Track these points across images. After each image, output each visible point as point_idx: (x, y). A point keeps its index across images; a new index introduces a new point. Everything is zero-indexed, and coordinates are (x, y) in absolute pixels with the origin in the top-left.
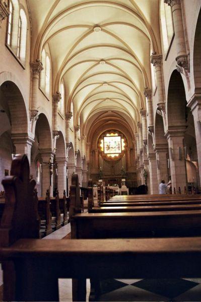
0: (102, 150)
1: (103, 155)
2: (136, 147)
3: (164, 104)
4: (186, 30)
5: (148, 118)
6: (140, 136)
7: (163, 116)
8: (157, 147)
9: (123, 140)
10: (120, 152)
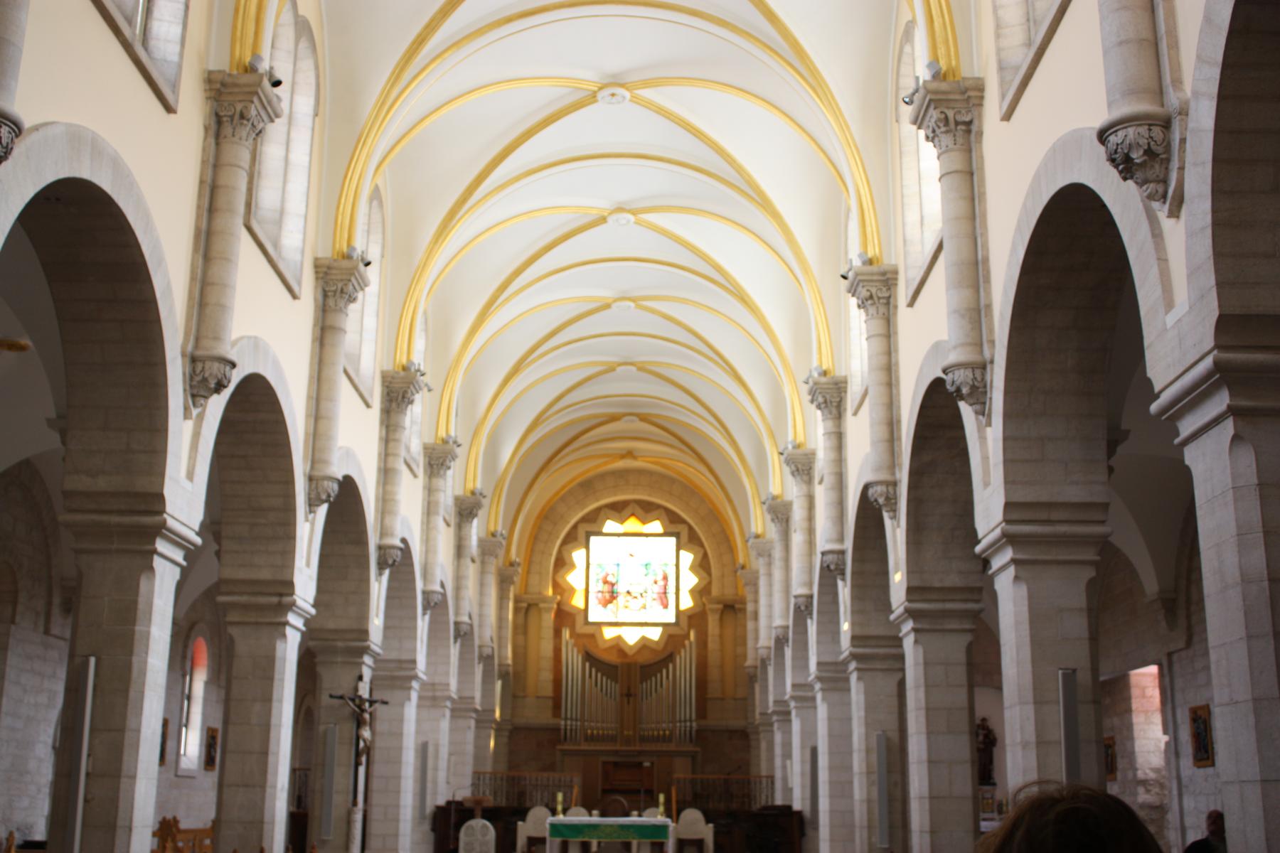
0: (578, 601)
1: (580, 628)
2: (756, 601)
3: (895, 484)
4: (986, 260)
5: (822, 495)
9: (687, 558)
10: (671, 618)
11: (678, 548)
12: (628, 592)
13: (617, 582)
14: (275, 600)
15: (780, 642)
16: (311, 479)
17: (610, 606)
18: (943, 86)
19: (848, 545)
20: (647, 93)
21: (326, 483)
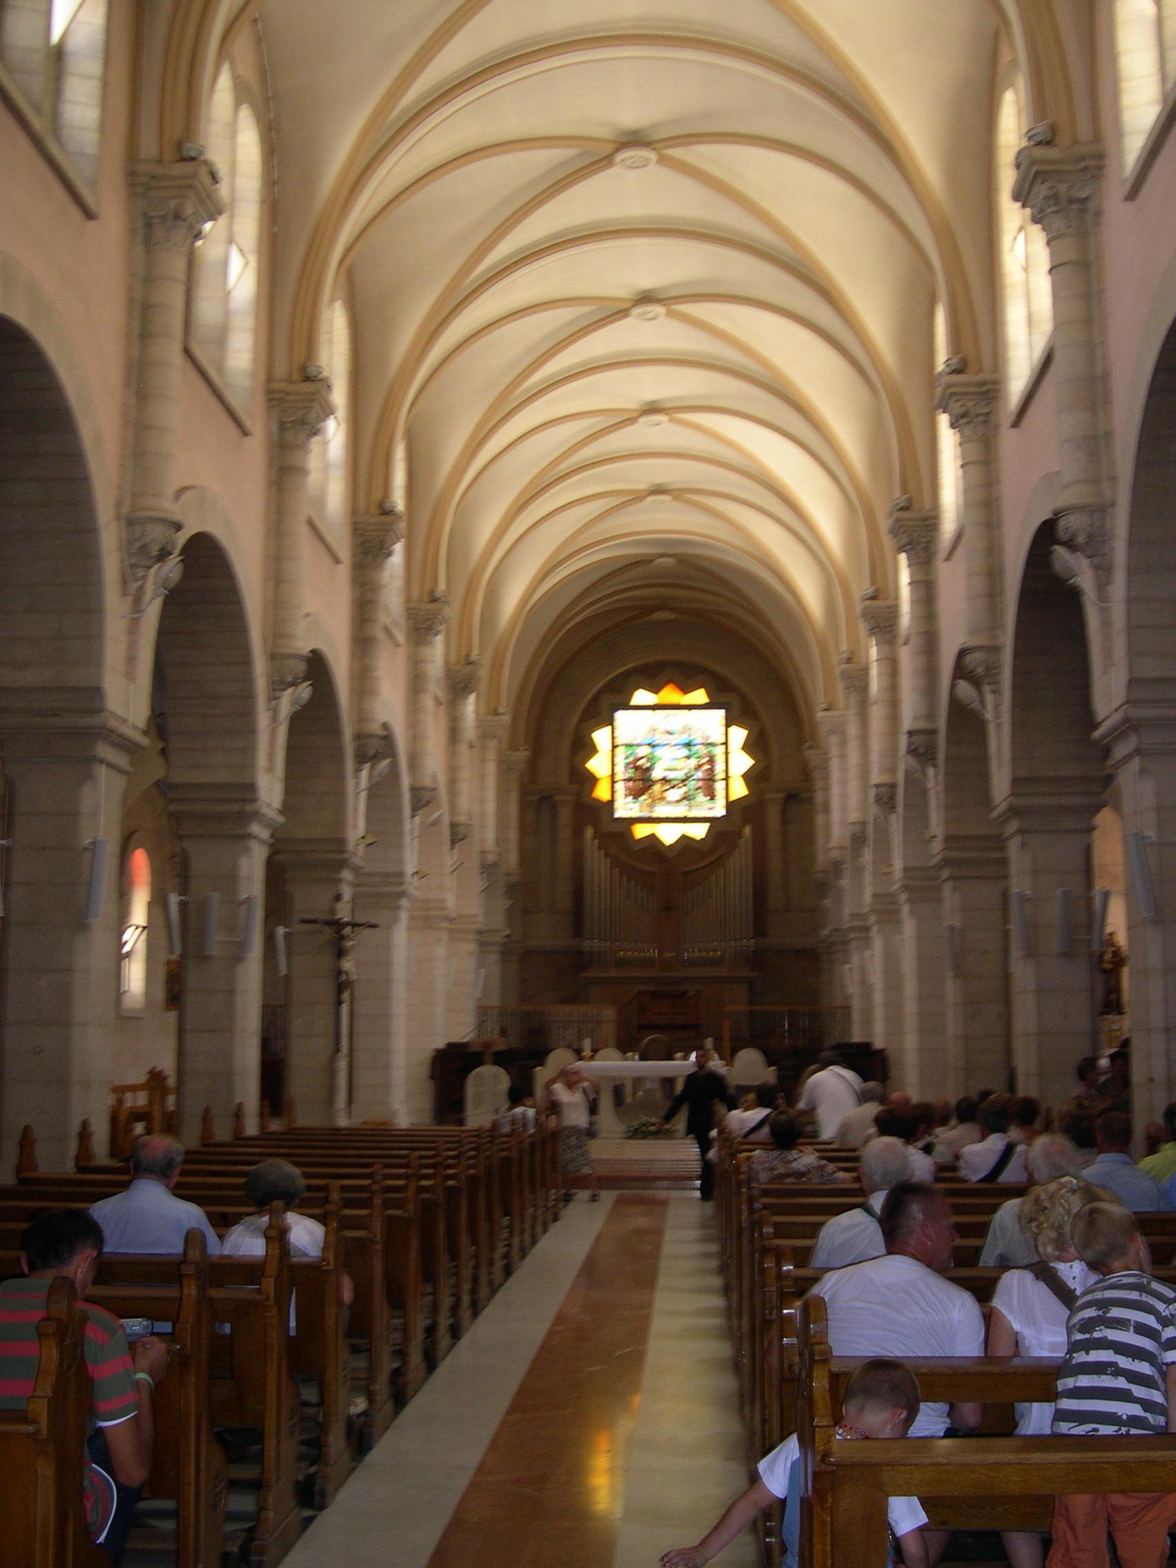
0: (602, 792)
2: (827, 789)
4: (1105, 376)
5: (907, 659)
6: (853, 730)
7: (989, 715)
8: (953, 854)
9: (739, 735)
10: (719, 810)
11: (728, 725)
12: (665, 780)
14: (236, 807)
15: (858, 840)
16: (273, 657)
18: (1052, 153)
19: (942, 723)
20: (677, 153)
21: (292, 662)
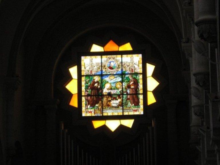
0: (74, 102)
9: (150, 68)
12: (109, 94)
13: (102, 88)
17: (97, 105)
